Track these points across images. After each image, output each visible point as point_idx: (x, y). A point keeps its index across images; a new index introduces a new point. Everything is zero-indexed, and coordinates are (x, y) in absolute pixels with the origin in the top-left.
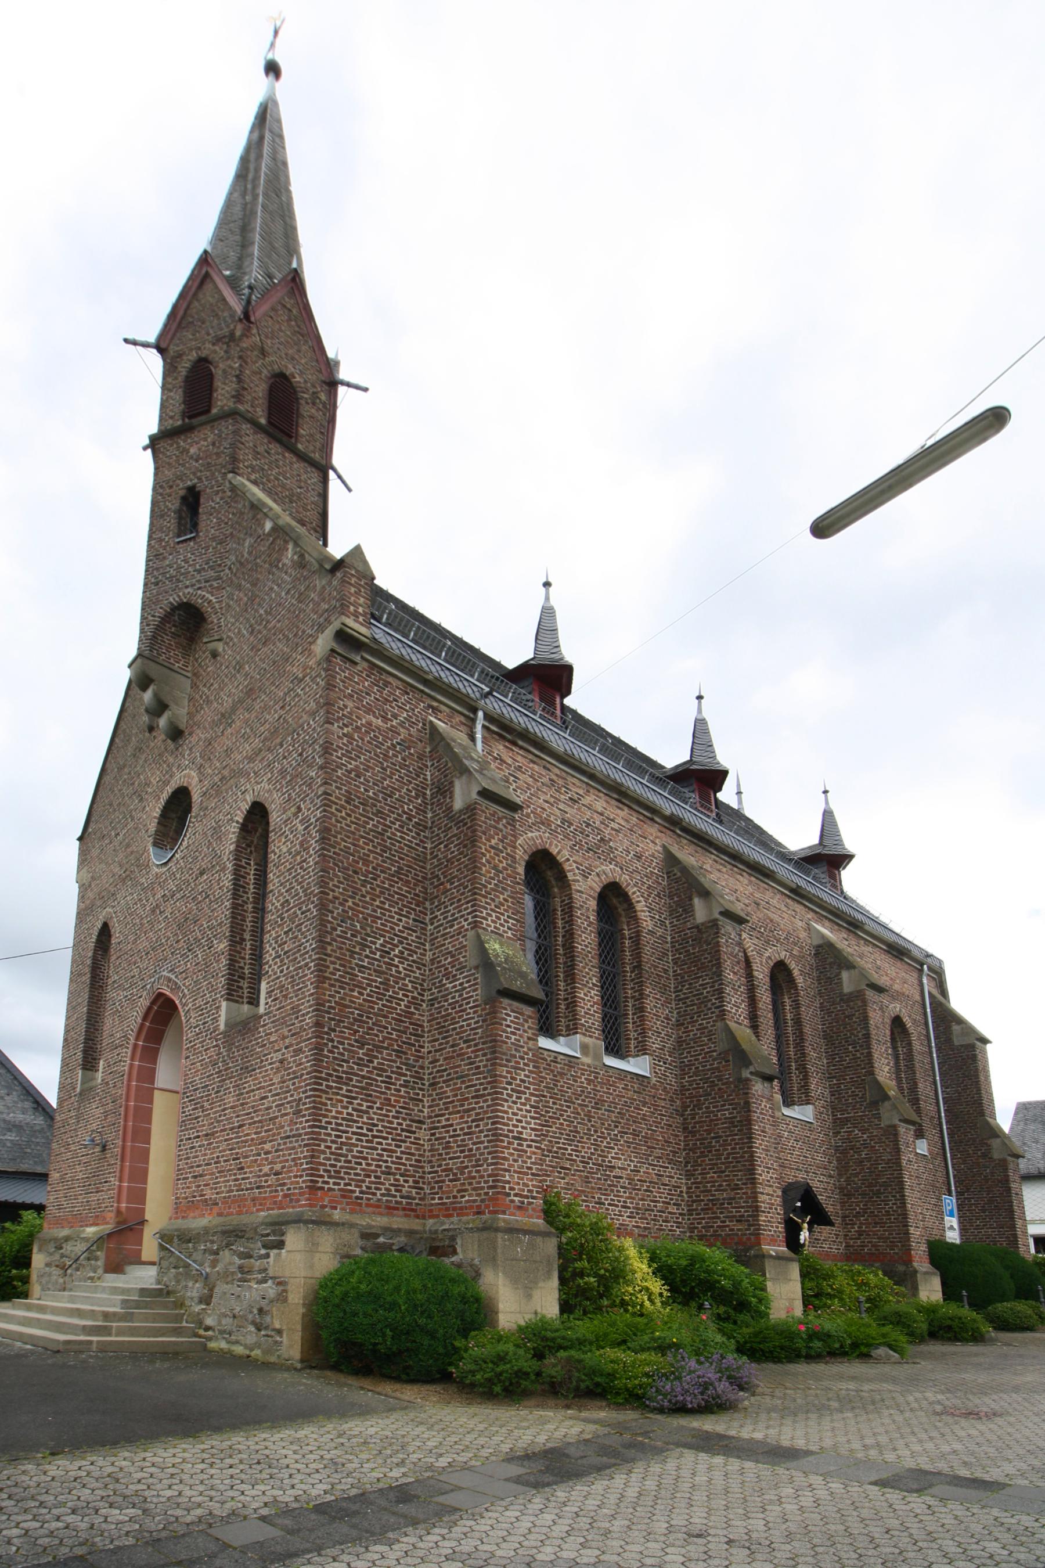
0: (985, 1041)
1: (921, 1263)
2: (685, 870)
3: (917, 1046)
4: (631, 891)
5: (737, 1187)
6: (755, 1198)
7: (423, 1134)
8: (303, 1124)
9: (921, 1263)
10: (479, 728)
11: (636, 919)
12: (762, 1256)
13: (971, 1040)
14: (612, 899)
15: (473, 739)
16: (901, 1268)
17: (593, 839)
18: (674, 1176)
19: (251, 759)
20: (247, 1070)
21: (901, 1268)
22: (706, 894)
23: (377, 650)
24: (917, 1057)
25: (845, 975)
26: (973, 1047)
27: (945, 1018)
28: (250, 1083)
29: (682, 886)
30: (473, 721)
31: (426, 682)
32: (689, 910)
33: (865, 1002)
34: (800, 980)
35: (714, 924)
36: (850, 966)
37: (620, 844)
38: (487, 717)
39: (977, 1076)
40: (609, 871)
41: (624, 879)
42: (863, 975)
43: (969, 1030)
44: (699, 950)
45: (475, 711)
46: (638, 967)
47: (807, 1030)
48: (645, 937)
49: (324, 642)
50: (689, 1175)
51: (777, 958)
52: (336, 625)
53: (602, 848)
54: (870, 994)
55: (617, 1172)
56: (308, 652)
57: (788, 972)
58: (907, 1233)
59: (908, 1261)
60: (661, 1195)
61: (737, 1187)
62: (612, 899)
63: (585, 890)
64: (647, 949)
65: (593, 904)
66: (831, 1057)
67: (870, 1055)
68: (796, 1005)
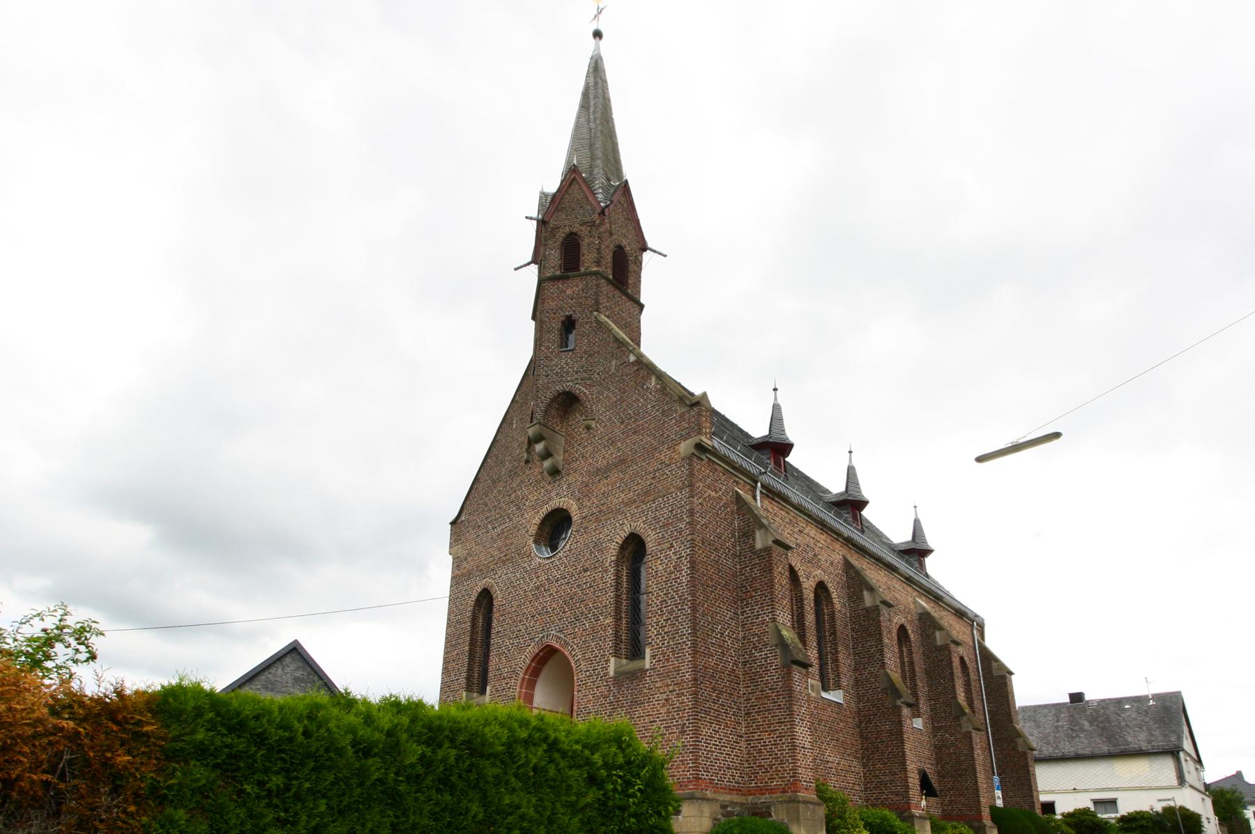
0: (1011, 673)
1: (987, 821)
2: (857, 573)
3: (973, 676)
4: (829, 585)
5: (895, 774)
6: (906, 781)
7: (743, 744)
8: (688, 739)
9: (987, 821)
10: (758, 493)
11: (832, 603)
12: (912, 817)
13: (1004, 673)
14: (821, 587)
15: (754, 498)
16: (976, 824)
17: (811, 554)
18: (857, 766)
19: (626, 505)
20: (635, 703)
21: (976, 824)
22: (871, 589)
23: (714, 452)
24: (973, 683)
25: (938, 634)
26: (1004, 677)
27: (988, 658)
28: (639, 711)
29: (856, 583)
30: (755, 488)
31: (734, 468)
32: (861, 598)
33: (950, 651)
34: (912, 636)
35: (877, 608)
36: (941, 628)
37: (823, 557)
38: (763, 486)
39: (1007, 696)
40: (819, 574)
41: (826, 578)
42: (948, 635)
43: (1002, 667)
44: (868, 622)
45: (756, 482)
46: (834, 633)
47: (917, 669)
48: (838, 615)
49: (685, 447)
50: (864, 766)
51: (900, 622)
52: (696, 439)
53: (814, 561)
54: (952, 646)
55: (830, 765)
56: (672, 448)
57: (906, 631)
58: (979, 801)
59: (980, 819)
60: (851, 778)
61: (895, 774)
62: (821, 587)
63: (808, 586)
64: (838, 622)
65: (812, 596)
66: (930, 686)
67: (954, 686)
68: (910, 653)
